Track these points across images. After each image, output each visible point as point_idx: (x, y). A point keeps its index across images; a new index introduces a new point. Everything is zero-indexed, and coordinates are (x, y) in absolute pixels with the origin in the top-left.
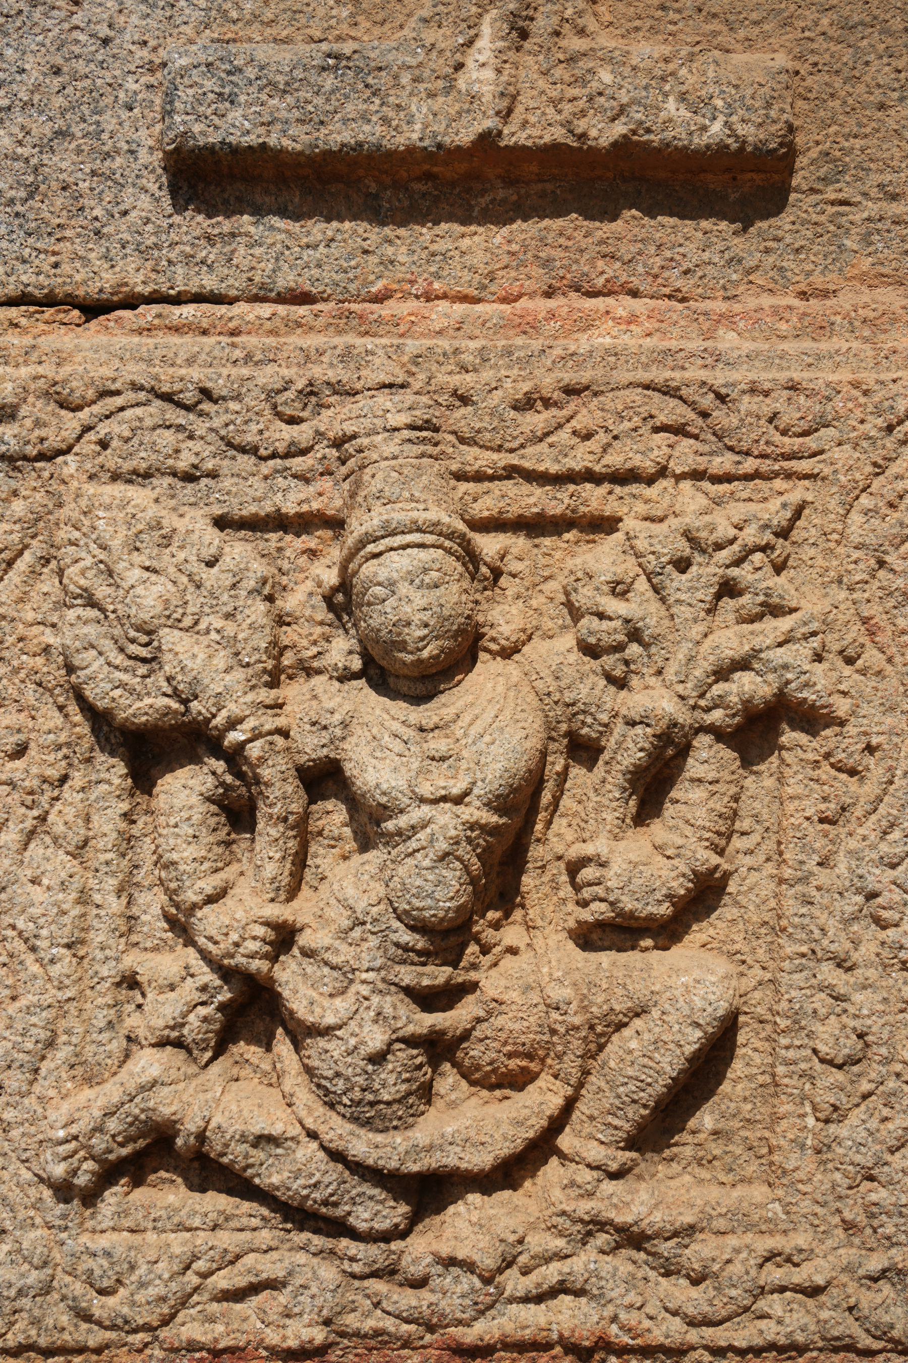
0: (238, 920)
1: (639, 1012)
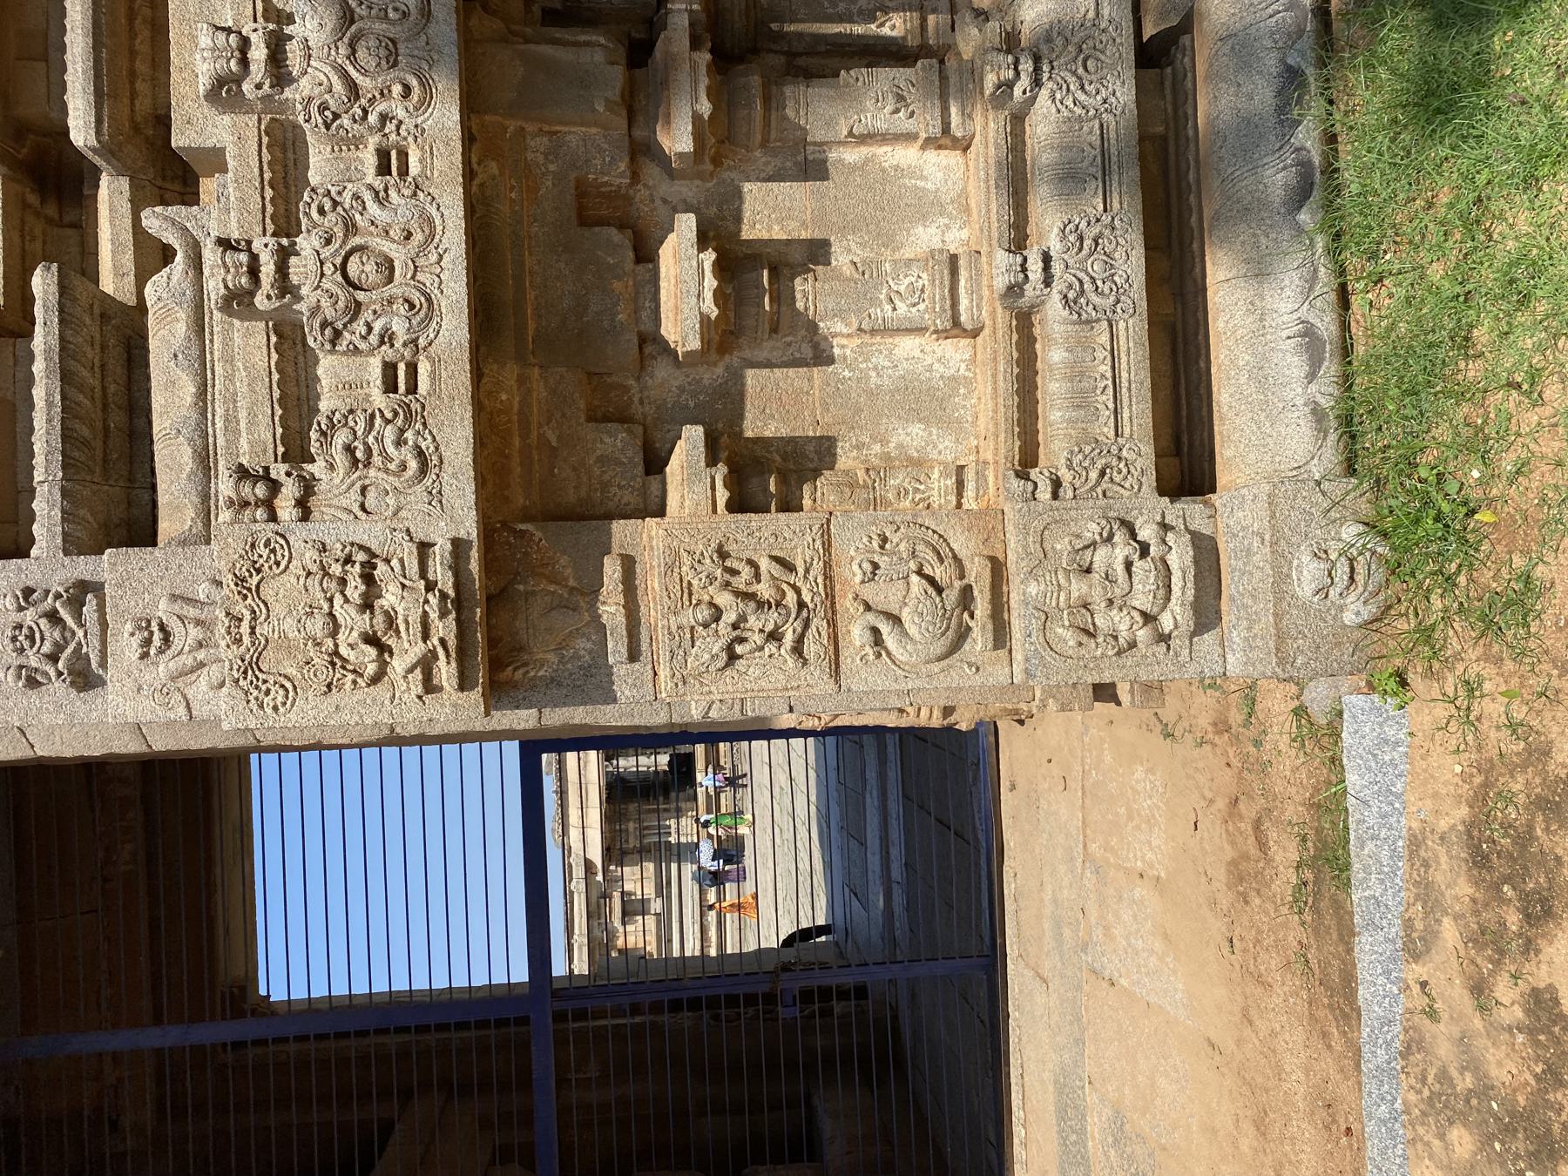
0: (758, 639)
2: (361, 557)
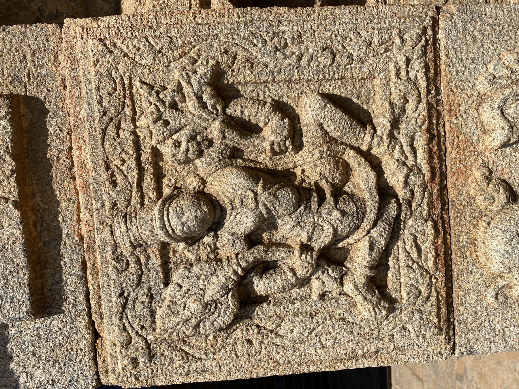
0: (298, 263)
1: (321, 126)
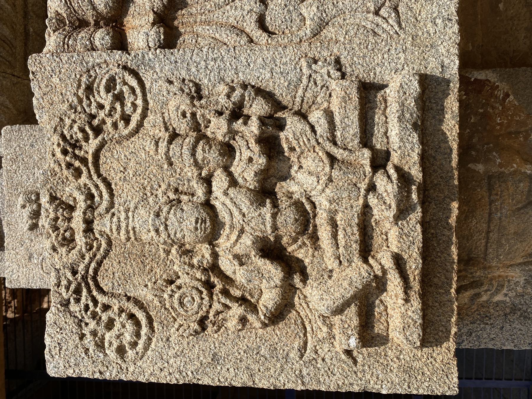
2: (257, 108)
